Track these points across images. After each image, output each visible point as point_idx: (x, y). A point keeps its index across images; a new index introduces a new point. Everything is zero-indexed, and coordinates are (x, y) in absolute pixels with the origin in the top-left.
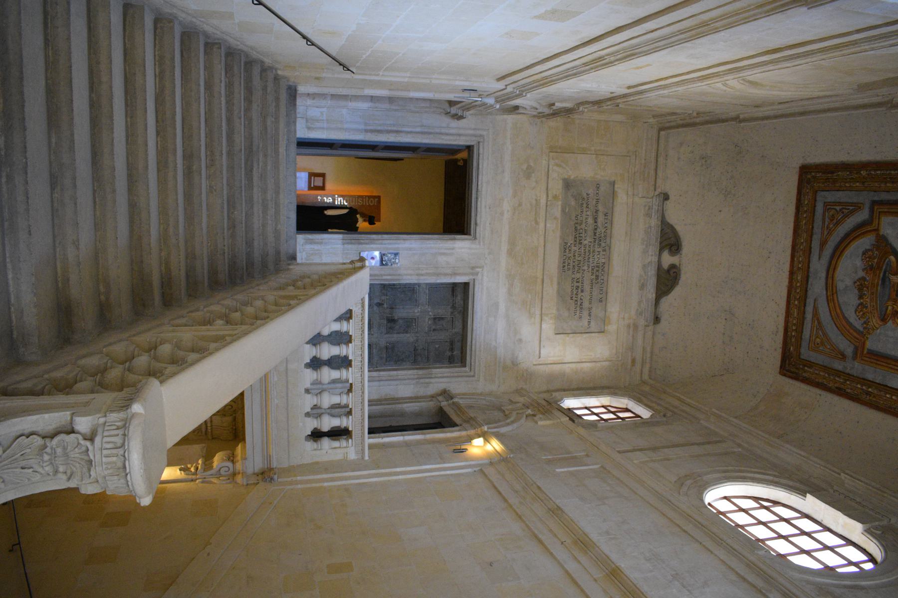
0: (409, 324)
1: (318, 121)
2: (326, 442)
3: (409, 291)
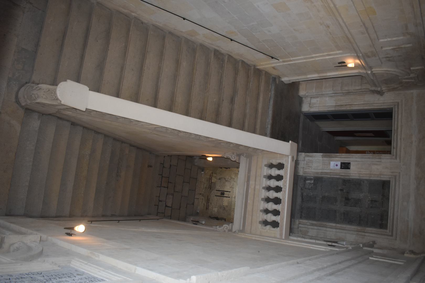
0: (357, 202)
1: (315, 104)
2: (268, 227)
3: (357, 184)
